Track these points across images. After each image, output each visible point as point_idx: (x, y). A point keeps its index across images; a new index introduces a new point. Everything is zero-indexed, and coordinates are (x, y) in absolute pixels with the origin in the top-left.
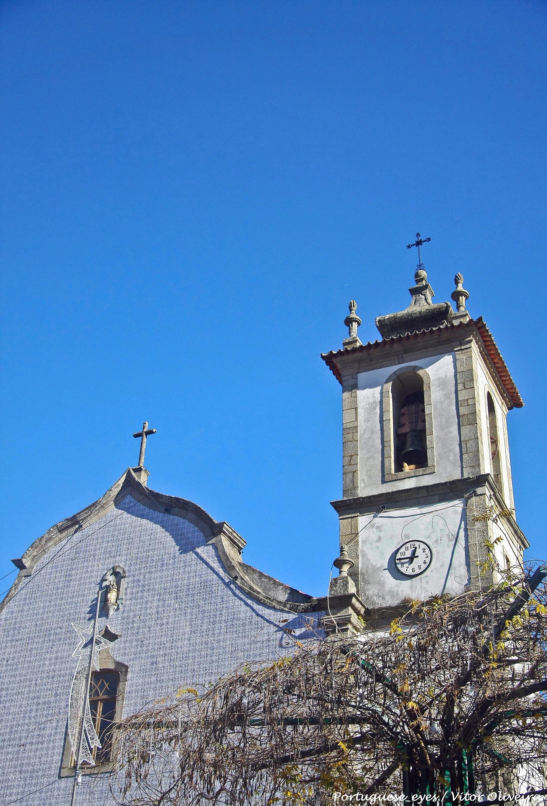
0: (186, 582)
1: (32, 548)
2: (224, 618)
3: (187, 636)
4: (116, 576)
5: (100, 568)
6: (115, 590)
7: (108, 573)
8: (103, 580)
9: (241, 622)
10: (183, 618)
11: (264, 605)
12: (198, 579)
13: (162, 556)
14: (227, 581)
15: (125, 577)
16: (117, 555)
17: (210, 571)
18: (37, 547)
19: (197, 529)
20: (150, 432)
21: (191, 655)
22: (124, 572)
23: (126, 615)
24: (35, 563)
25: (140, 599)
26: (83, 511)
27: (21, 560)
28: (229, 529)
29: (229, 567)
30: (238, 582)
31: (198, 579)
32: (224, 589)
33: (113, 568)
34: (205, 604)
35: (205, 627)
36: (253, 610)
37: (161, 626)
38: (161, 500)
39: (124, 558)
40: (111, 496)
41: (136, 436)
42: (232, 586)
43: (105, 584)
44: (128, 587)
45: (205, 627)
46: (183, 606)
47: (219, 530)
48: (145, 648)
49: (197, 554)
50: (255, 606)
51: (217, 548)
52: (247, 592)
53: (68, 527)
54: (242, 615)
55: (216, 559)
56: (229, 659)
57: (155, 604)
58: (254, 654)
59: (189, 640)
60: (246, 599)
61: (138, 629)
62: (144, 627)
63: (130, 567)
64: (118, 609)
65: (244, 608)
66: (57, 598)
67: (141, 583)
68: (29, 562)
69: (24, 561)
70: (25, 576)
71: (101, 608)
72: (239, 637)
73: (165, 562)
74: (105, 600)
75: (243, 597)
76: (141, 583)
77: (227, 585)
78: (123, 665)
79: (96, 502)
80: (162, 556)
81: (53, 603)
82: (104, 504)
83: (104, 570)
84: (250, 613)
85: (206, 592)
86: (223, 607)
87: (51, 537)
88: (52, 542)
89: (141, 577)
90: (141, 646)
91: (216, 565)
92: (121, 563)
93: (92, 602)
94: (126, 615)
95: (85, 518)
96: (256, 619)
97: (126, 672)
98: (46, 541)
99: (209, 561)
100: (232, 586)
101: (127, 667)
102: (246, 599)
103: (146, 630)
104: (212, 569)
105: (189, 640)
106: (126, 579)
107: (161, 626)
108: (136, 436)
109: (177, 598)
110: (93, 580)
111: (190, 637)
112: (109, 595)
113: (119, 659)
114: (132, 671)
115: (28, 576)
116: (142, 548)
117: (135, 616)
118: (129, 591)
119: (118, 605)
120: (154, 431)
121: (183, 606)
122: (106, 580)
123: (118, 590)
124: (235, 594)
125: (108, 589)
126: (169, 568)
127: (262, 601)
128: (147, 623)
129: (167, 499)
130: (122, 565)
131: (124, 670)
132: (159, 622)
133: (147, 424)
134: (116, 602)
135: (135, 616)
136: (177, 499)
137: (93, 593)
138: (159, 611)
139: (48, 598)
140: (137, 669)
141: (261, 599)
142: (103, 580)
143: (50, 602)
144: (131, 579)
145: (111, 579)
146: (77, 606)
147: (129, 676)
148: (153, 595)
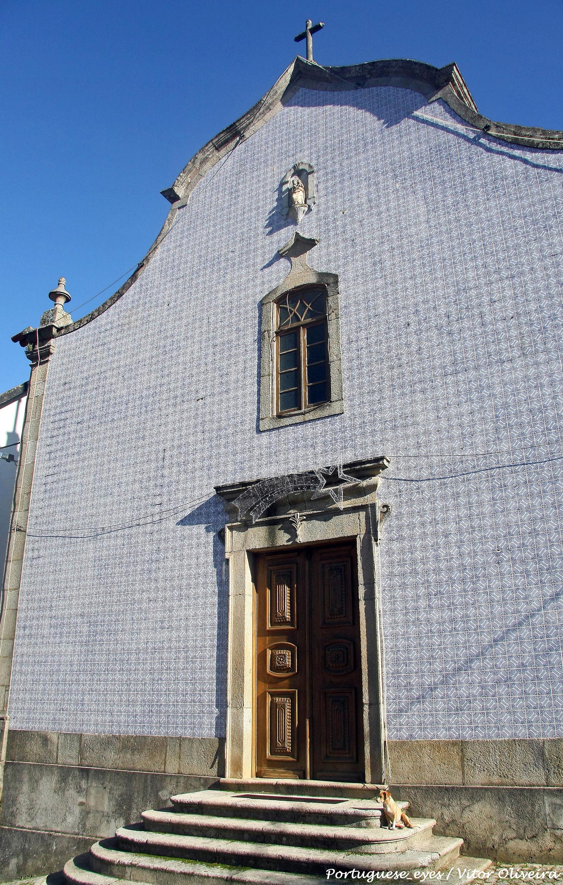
0: (406, 154)
1: (184, 173)
2: (478, 182)
3: (422, 219)
4: (299, 176)
5: (277, 171)
6: (301, 188)
7: (288, 175)
8: (282, 183)
9: (510, 181)
10: (411, 198)
11: (545, 149)
12: (424, 147)
13: (363, 134)
14: (472, 136)
15: (313, 172)
16: (296, 152)
17: (441, 132)
18: (190, 171)
19: (408, 91)
20: (316, 29)
21: (435, 240)
22: (310, 167)
23: (322, 215)
24: (190, 191)
25: (340, 191)
26: (243, 117)
27: (172, 188)
28: (459, 78)
29: (472, 118)
30: (493, 132)
31: (424, 147)
32: (469, 147)
33: (294, 167)
34: (444, 172)
35: (450, 201)
36: (525, 162)
37: (379, 215)
38: (348, 76)
39: (306, 153)
40: (278, 93)
41: (298, 39)
42: (482, 141)
43: (285, 188)
44: (319, 183)
45: (450, 201)
46: (408, 183)
47: (446, 78)
48: (358, 248)
49: (416, 119)
50: (529, 156)
51: (446, 102)
52: (509, 140)
53: (226, 142)
54: (510, 172)
55: (447, 115)
56: (502, 232)
57: (364, 192)
58: (543, 217)
59: (428, 222)
60: (510, 151)
61: (344, 227)
62: (353, 222)
63: (318, 160)
64: (310, 210)
65: (509, 162)
66: (223, 220)
67: (338, 173)
68: (183, 192)
69: (176, 189)
70: (179, 208)
71: (285, 212)
72: (511, 200)
73: (369, 140)
74: (291, 202)
75: (505, 149)
76: (338, 173)
77: (475, 142)
78: (328, 275)
79: (260, 102)
80: (363, 134)
81: (218, 227)
82: (271, 104)
83: (281, 173)
84: (521, 167)
85: (441, 157)
86: (474, 170)
87: (207, 158)
88: (209, 164)
89: (337, 166)
90: (353, 246)
91: (450, 123)
92: (304, 159)
93: (270, 213)
94: (322, 215)
95: (247, 126)
96: (533, 172)
97: (336, 282)
98: (201, 164)
99: (439, 121)
100: (482, 141)
101: (336, 276)
102: (510, 151)
103: (356, 226)
104: (445, 129)
105: (428, 222)
106: (315, 175)
107: (379, 215)
108: (298, 39)
109: (396, 176)
110: (268, 187)
111: (429, 218)
112: (294, 196)
113: (323, 269)
114: (344, 280)
115: (183, 207)
116: (331, 135)
117: (336, 213)
118: (321, 186)
119: (309, 206)
120: (321, 24)
121: (408, 183)
122: (287, 182)
123: (306, 189)
124: (489, 150)
125: (291, 191)
126: (376, 146)
127: (541, 146)
128: (357, 217)
129: (358, 68)
130: (305, 161)
131: (331, 280)
132: (374, 211)
133: (310, 22)
134: (306, 203)
135: (336, 213)
136: (373, 64)
137: (270, 203)
138: (371, 198)
139: (212, 223)
140: (351, 275)
141: (538, 144)
142: (282, 183)
143: (214, 226)
144: (321, 172)
145: (292, 180)
146: (251, 222)
147: (341, 286)
148: (360, 182)
